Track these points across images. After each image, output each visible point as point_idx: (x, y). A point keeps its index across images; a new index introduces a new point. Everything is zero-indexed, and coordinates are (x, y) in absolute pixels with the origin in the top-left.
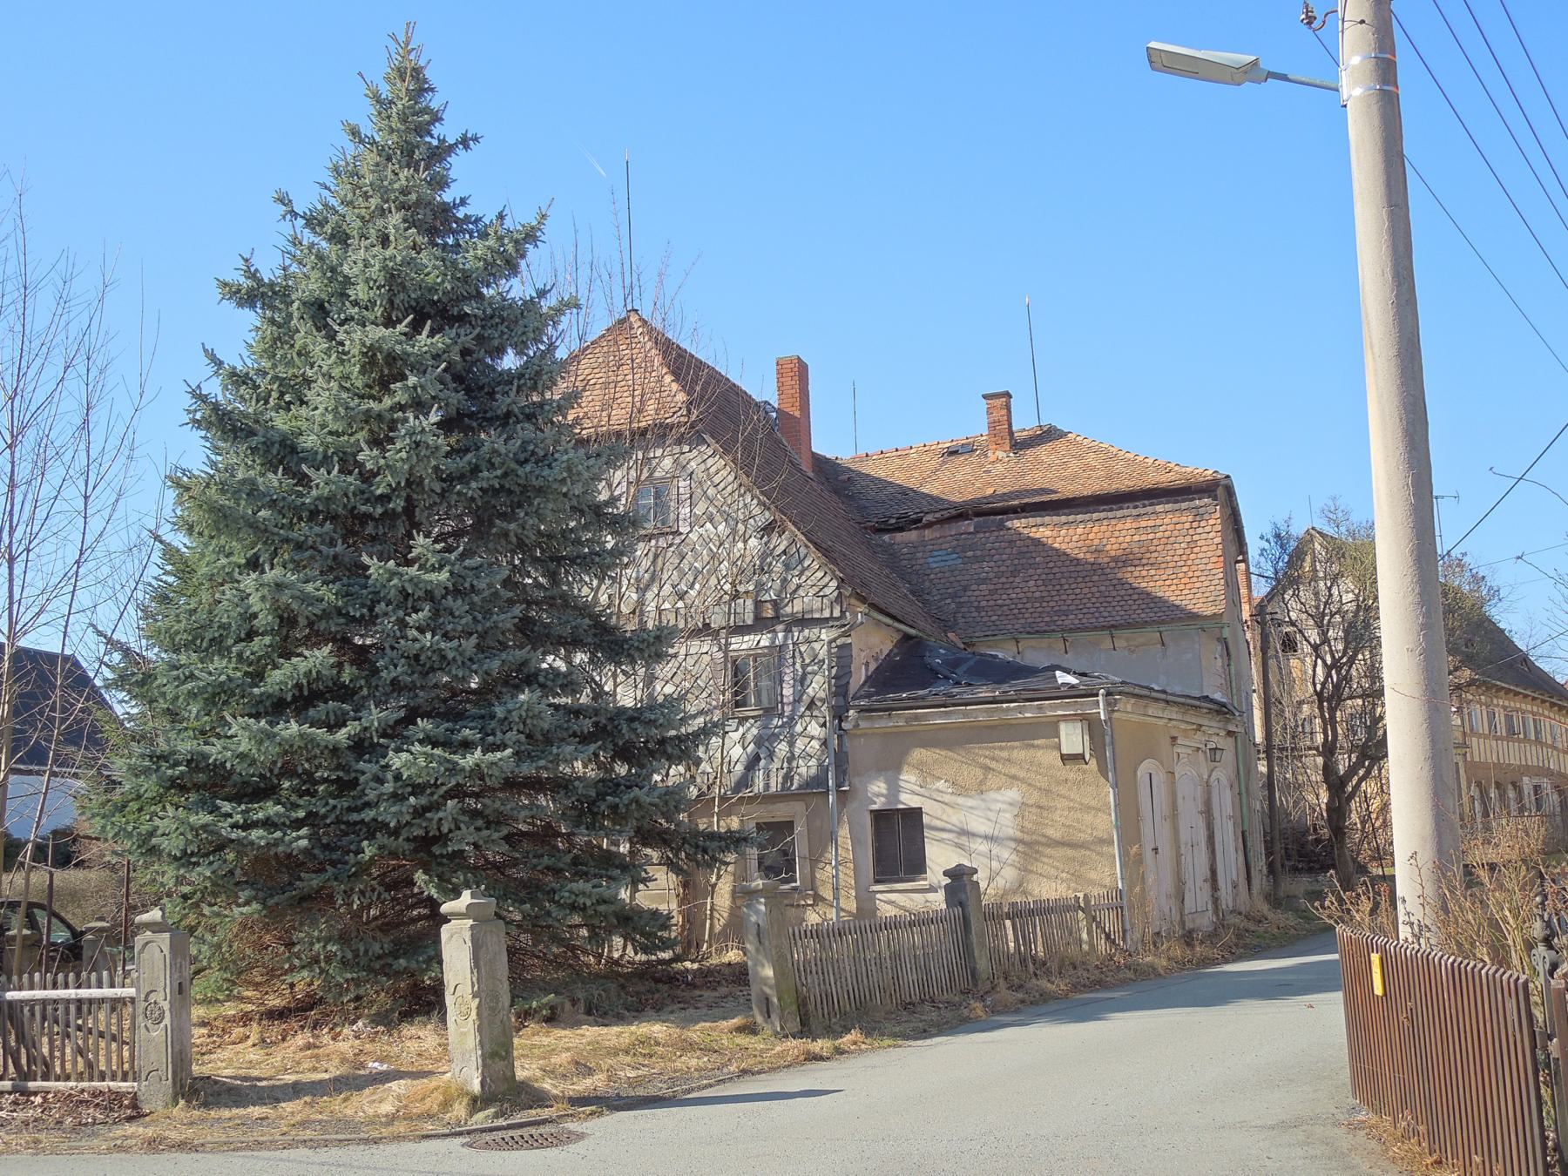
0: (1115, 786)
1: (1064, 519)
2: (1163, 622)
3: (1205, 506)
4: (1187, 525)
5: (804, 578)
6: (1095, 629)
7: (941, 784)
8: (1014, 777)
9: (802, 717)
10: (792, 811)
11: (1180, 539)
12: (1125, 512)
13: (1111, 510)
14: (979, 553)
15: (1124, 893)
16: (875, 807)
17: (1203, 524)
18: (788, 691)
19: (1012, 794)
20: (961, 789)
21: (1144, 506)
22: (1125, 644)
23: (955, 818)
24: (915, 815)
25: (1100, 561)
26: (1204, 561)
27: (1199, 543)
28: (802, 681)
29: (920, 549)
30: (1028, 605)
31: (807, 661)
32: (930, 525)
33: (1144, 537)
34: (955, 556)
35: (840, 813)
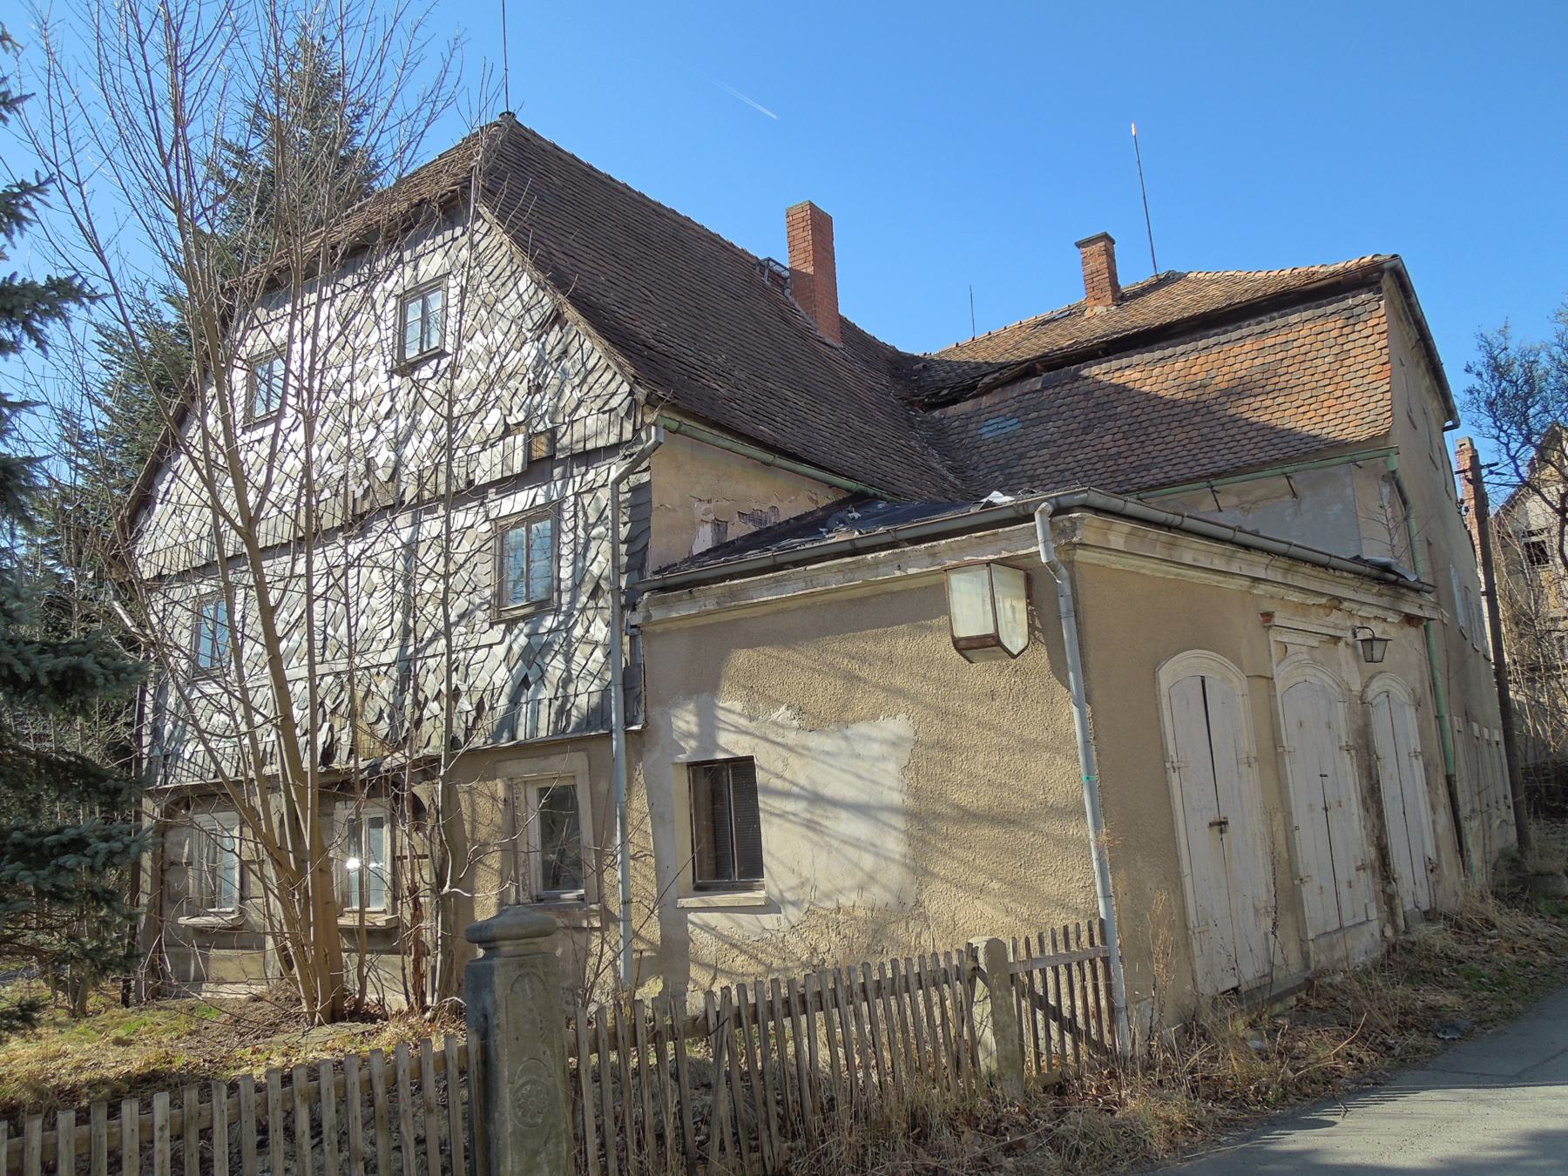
0: (1086, 697)
1: (1158, 354)
2: (1288, 460)
3: (1363, 304)
4: (1335, 333)
5: (585, 388)
6: (1189, 481)
7: (781, 714)
8: (900, 693)
9: (583, 610)
10: (568, 767)
11: (1325, 352)
12: (1245, 331)
13: (1225, 332)
14: (1044, 413)
15: (1113, 928)
16: (682, 758)
17: (1358, 328)
18: (566, 573)
19: (897, 726)
20: (812, 721)
21: (1273, 319)
22: (1235, 501)
23: (801, 773)
24: (744, 767)
25: (1204, 398)
26: (1360, 374)
27: (1353, 353)
28: (580, 554)
29: (974, 420)
30: (1099, 465)
31: (592, 520)
32: (988, 390)
33: (1270, 359)
34: (1015, 420)
35: (631, 769)
